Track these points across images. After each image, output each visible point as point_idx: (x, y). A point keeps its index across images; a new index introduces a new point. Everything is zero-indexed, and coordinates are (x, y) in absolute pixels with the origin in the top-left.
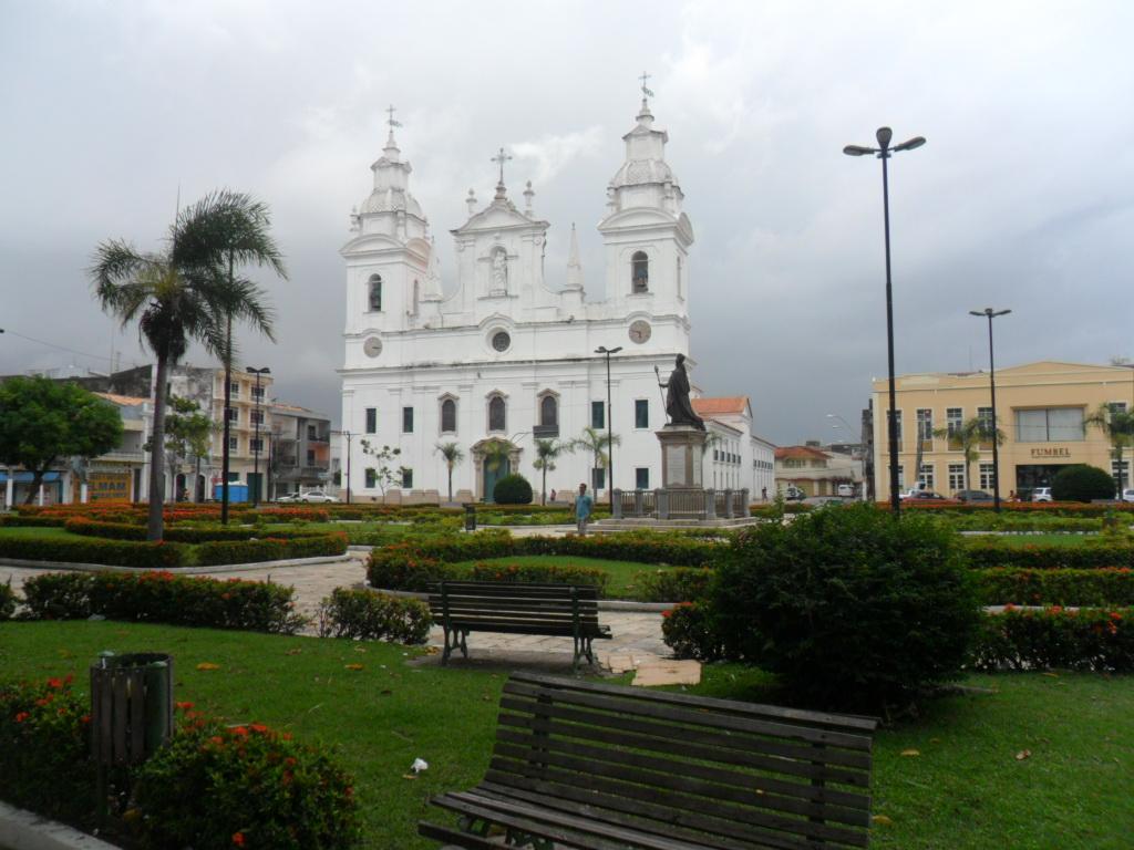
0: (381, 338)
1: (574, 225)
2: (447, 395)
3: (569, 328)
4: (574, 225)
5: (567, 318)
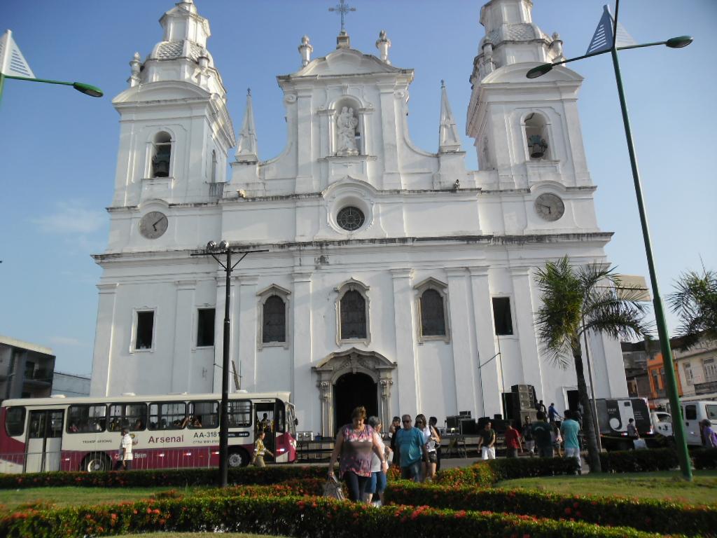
0: (167, 213)
1: (442, 82)
2: (274, 288)
3: (453, 194)
4: (442, 82)
5: (449, 181)
